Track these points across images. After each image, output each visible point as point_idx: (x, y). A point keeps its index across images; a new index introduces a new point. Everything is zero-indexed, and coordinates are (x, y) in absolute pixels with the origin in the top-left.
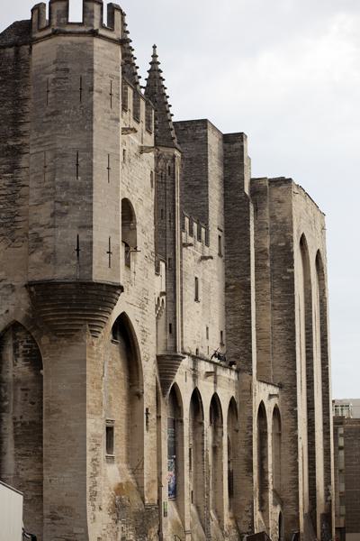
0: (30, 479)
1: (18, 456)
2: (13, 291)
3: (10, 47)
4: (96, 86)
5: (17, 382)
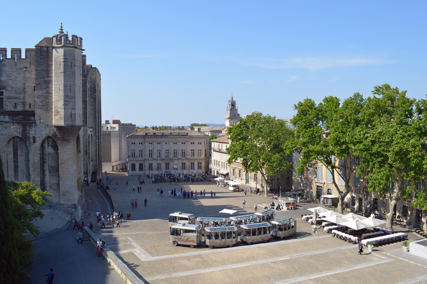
0: (54, 183)
1: (50, 176)
2: (48, 126)
3: (45, 47)
4: (76, 65)
5: (49, 154)
